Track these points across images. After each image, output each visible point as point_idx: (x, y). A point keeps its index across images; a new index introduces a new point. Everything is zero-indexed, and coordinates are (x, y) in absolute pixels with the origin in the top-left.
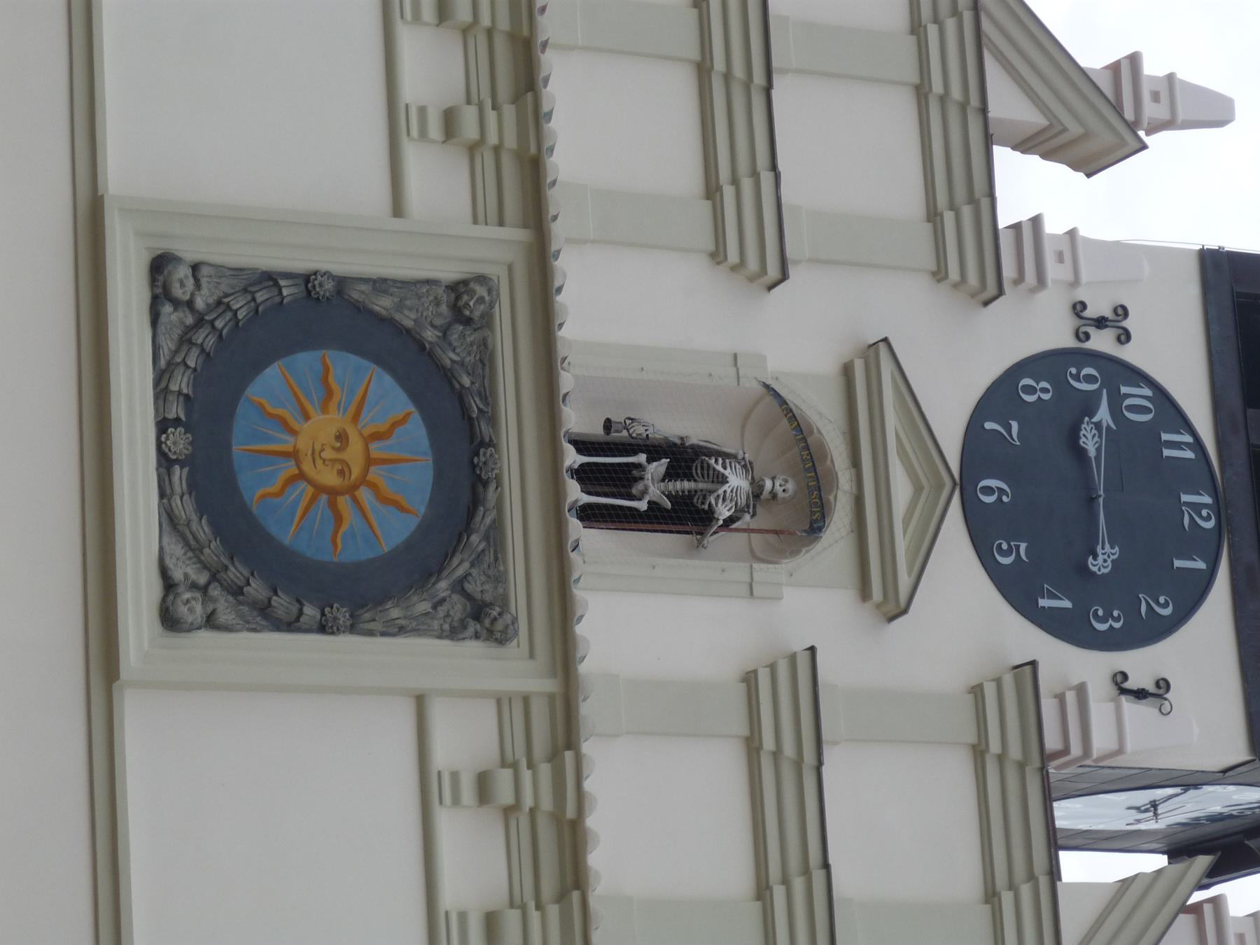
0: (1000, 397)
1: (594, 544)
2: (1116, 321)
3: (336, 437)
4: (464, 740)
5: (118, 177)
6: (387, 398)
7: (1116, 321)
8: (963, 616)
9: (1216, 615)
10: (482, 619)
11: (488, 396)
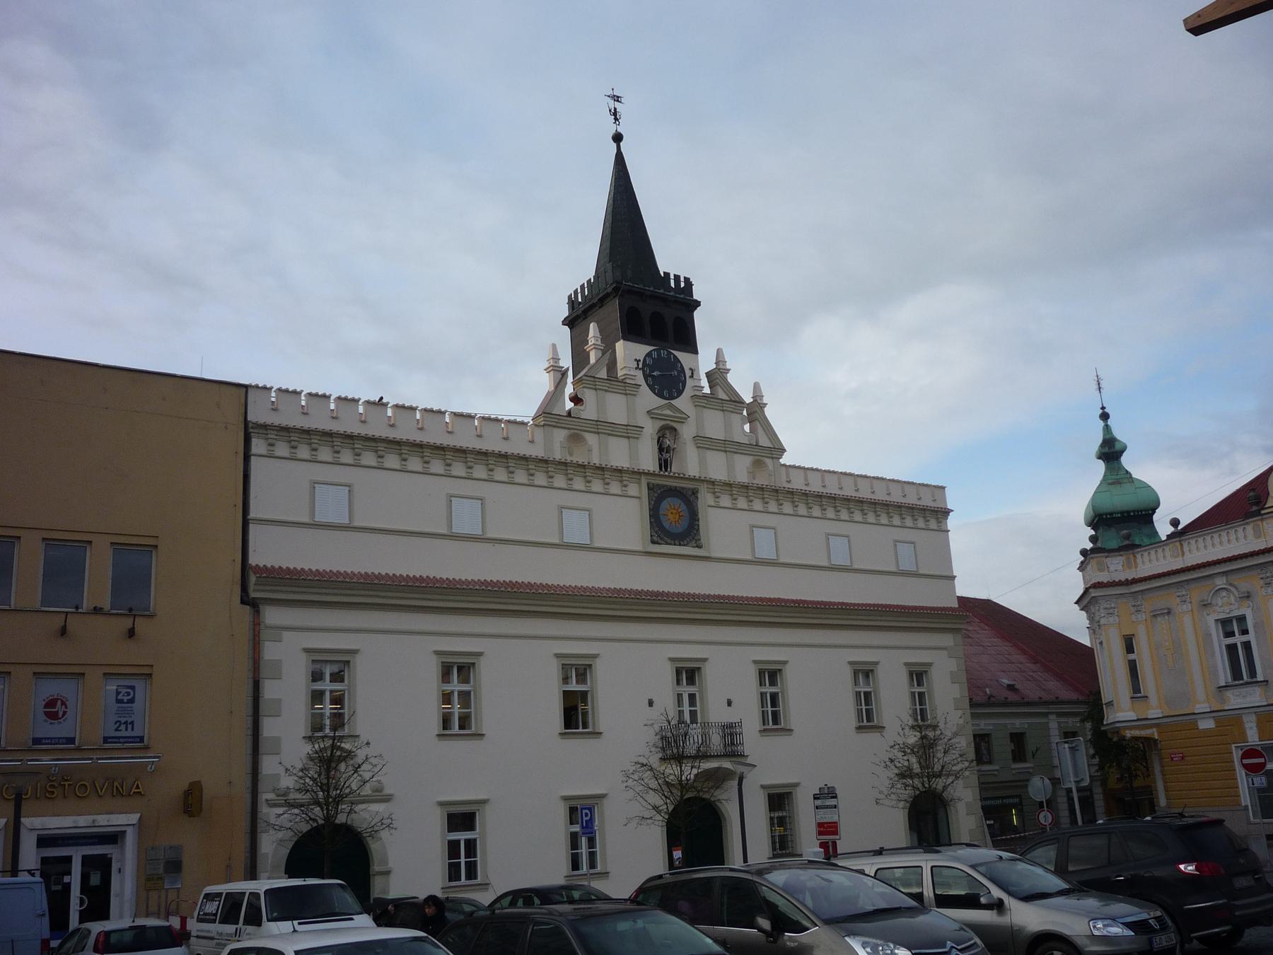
0: (652, 388)
1: (675, 468)
2: (638, 361)
3: (672, 512)
4: (710, 500)
5: (639, 548)
6: (665, 504)
7: (638, 361)
8: (683, 402)
9: (679, 355)
10: (695, 492)
11: (664, 486)
